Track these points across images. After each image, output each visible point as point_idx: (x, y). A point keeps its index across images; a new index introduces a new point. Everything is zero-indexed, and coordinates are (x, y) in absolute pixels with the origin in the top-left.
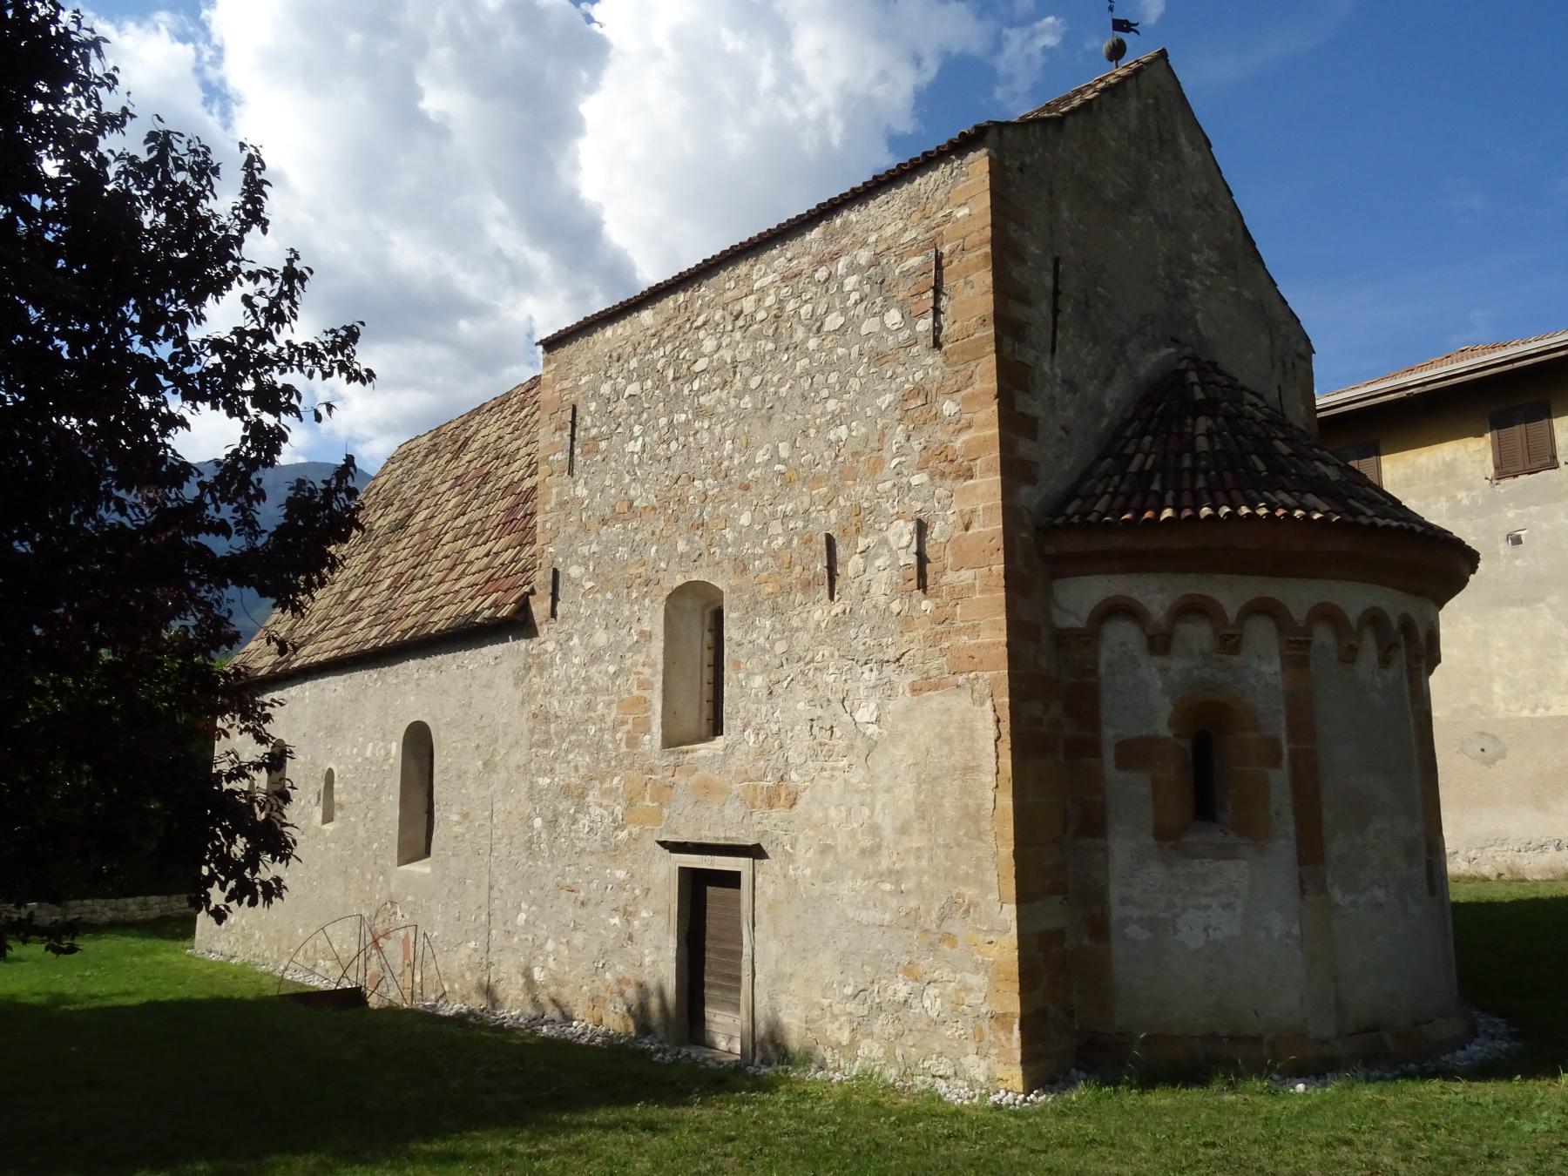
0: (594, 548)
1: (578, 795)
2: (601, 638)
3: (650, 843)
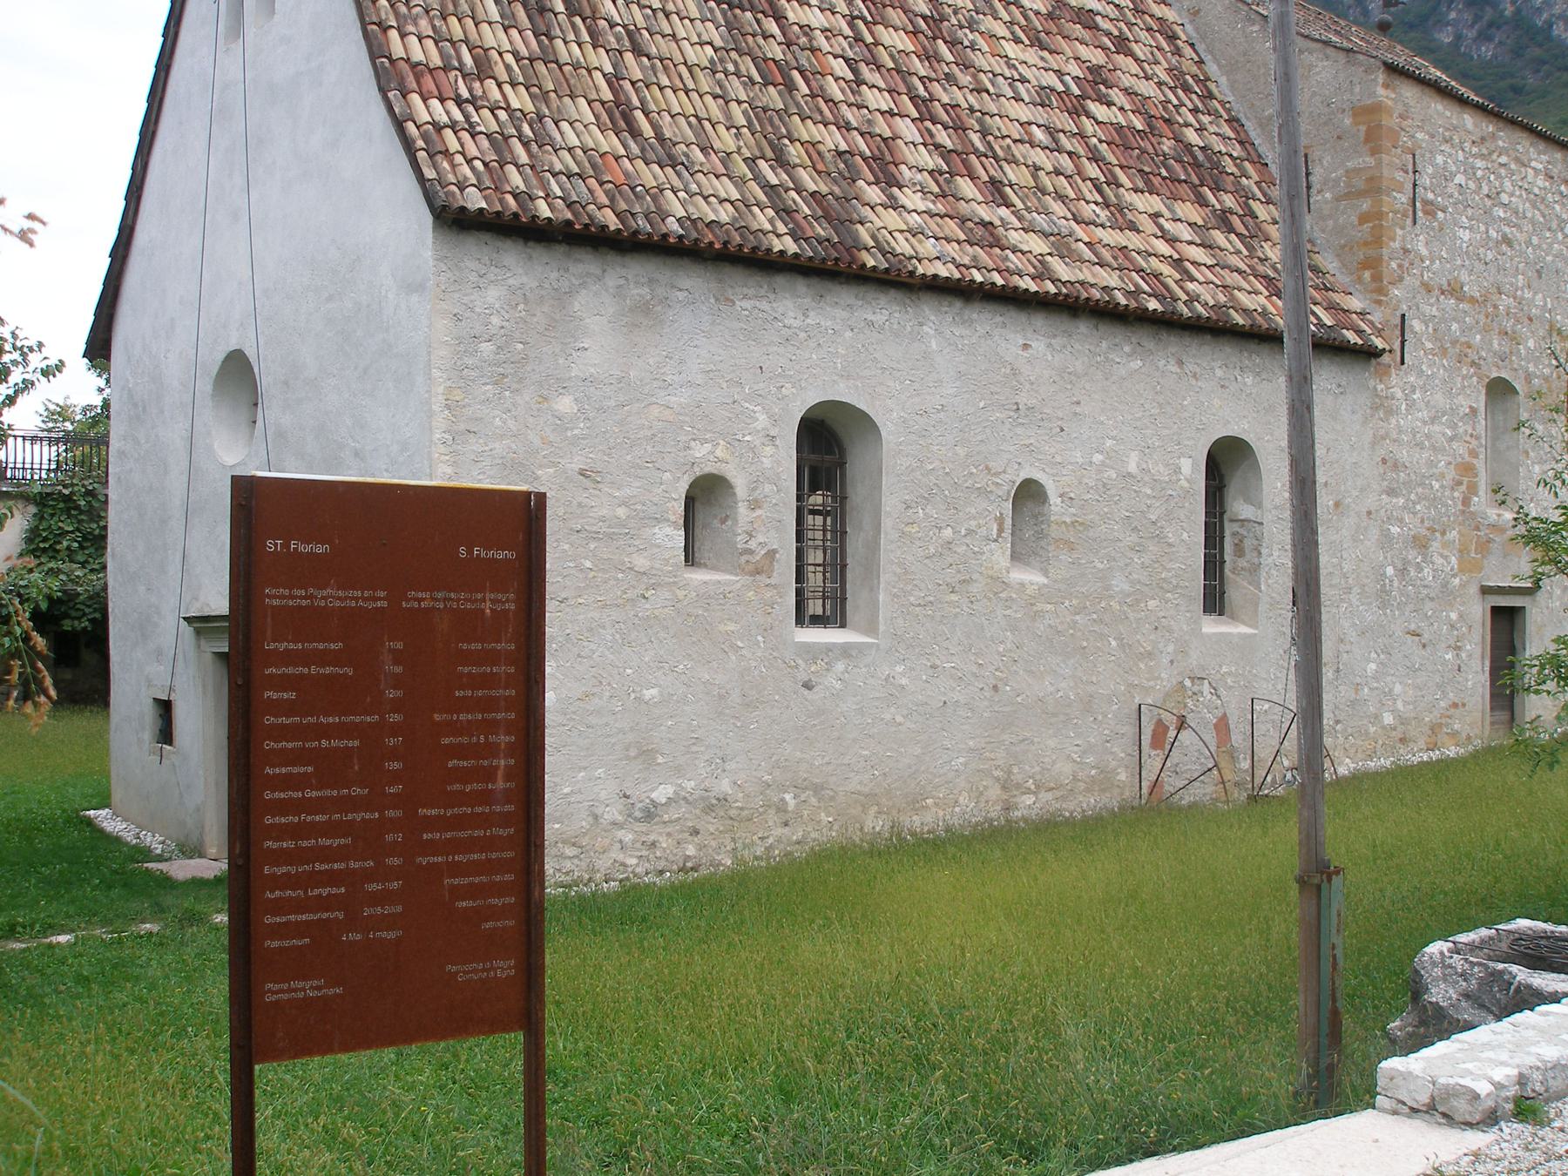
0: (1434, 312)
1: (1421, 544)
2: (1439, 399)
3: (1474, 590)
